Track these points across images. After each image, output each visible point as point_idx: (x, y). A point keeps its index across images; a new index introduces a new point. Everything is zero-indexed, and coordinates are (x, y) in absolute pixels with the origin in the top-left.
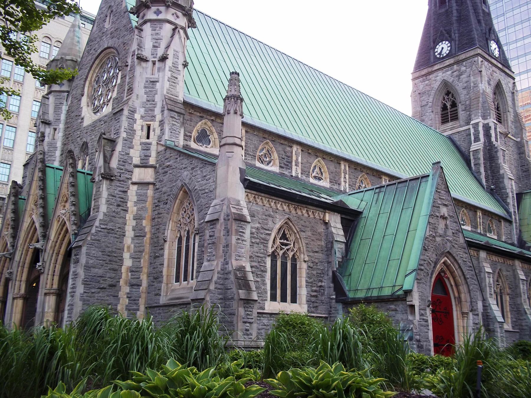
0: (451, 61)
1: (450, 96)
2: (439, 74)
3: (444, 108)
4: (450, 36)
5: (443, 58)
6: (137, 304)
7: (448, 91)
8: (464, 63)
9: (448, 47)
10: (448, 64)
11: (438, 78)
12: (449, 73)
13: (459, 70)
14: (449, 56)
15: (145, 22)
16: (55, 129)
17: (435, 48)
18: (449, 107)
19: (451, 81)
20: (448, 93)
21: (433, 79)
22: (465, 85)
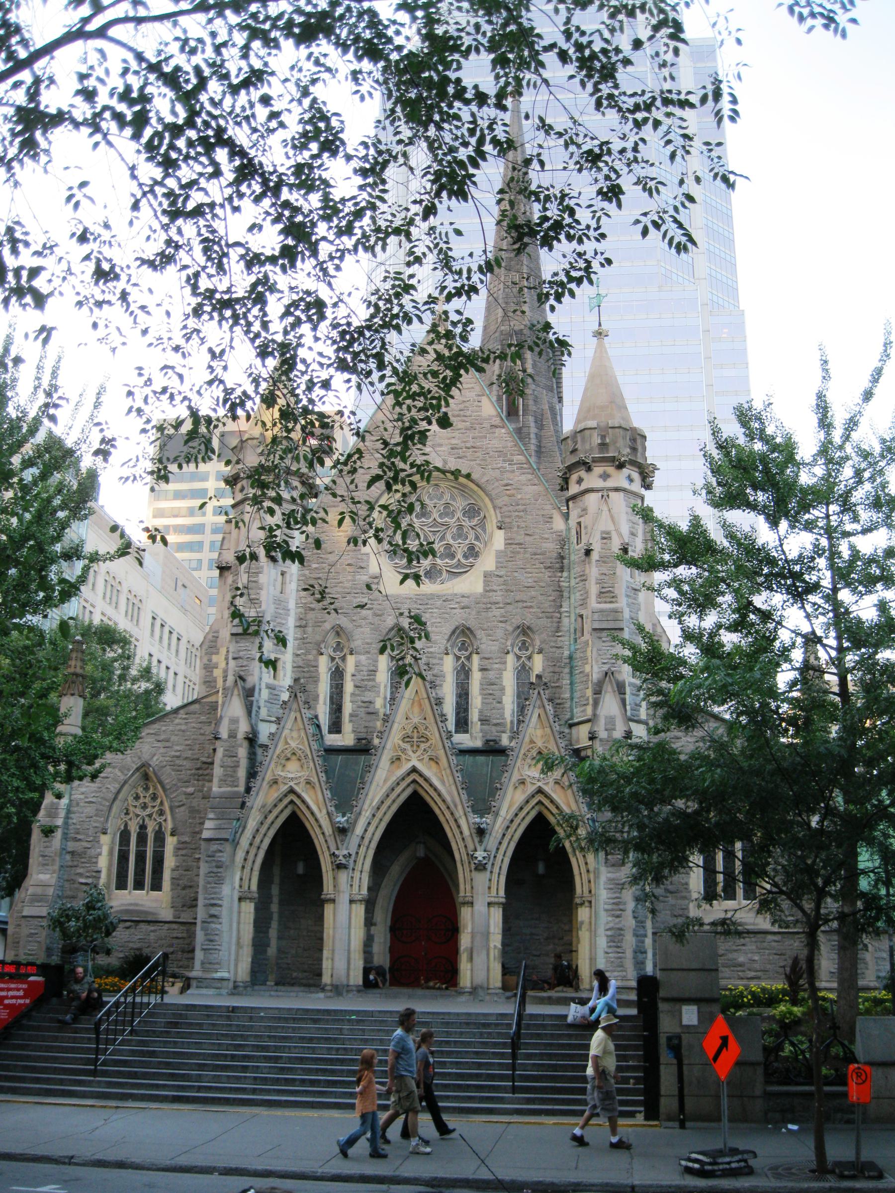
6: (644, 927)
15: (617, 490)
16: (283, 574)
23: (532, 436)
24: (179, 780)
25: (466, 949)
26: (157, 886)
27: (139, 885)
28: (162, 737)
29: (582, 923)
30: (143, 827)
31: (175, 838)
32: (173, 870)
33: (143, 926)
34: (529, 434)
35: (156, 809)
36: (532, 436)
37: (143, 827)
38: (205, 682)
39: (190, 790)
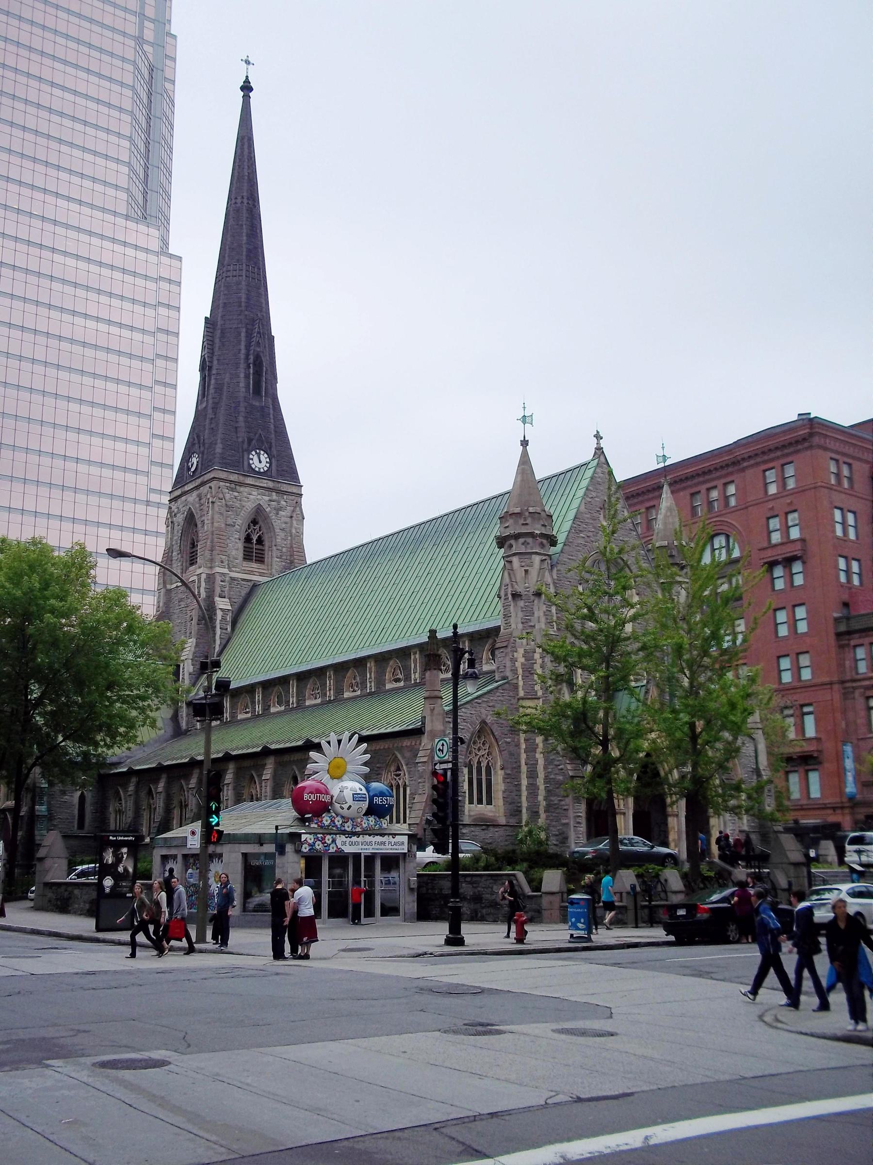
0: (270, 484)
1: (257, 527)
2: (254, 493)
3: (248, 539)
4: (270, 448)
5: (259, 473)
7: (255, 519)
8: (285, 497)
9: (267, 462)
10: (265, 485)
12: (267, 498)
13: (279, 502)
14: (266, 474)
17: (249, 453)
18: (254, 541)
20: (254, 522)
21: (245, 494)
22: (284, 526)
23: (271, 416)
24: (503, 733)
25: (674, 840)
26: (489, 802)
27: (480, 802)
28: (491, 704)
29: (713, 826)
30: (479, 763)
31: (503, 771)
32: (504, 792)
33: (491, 829)
34: (269, 414)
35: (487, 751)
36: (271, 416)
37: (479, 763)
38: (512, 670)
39: (508, 740)
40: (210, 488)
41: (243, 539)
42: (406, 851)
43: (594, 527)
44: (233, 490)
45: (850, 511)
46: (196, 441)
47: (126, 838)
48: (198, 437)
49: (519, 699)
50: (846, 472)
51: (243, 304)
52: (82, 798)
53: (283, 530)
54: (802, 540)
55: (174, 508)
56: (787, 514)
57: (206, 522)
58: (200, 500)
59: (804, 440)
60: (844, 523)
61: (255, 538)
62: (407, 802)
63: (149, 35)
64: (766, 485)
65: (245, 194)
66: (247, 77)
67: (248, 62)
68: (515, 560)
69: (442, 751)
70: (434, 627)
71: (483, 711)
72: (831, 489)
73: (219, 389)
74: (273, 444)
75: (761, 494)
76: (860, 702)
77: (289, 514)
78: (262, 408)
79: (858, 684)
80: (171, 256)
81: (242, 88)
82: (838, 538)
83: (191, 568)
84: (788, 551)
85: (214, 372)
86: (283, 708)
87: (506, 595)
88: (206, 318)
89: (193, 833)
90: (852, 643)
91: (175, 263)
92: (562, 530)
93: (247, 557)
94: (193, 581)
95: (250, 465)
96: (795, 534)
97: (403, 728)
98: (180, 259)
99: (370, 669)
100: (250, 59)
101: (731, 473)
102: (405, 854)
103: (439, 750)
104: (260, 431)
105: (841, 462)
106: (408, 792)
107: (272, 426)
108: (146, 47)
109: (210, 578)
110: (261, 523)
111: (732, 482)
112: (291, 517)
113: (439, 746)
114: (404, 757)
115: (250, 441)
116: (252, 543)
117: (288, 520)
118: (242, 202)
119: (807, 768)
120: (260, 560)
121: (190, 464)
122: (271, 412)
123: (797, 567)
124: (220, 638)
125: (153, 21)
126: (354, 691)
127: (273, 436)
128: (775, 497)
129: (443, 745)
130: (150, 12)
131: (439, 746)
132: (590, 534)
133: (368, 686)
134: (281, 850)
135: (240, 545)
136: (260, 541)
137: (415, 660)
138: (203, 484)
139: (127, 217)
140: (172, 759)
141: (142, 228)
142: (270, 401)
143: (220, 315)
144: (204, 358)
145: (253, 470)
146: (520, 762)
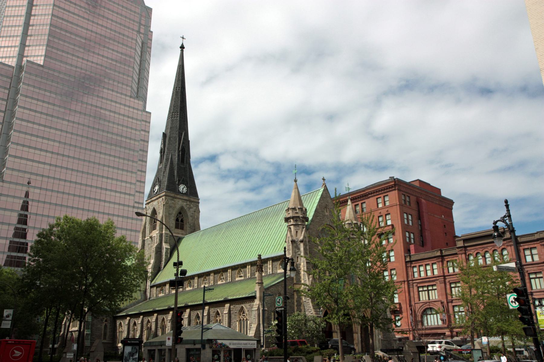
1: (181, 215)
2: (180, 201)
3: (177, 220)
4: (187, 184)
5: (182, 193)
7: (180, 212)
8: (193, 203)
11: (179, 203)
12: (185, 204)
13: (190, 205)
14: (186, 194)
18: (180, 221)
19: (185, 208)
20: (180, 213)
21: (177, 202)
22: (192, 215)
25: (356, 343)
34: (187, 170)
40: (163, 199)
41: (175, 220)
42: (256, 347)
43: (323, 215)
44: (171, 200)
45: (409, 214)
46: (157, 180)
47: (135, 342)
48: (158, 179)
49: (294, 284)
50: (408, 199)
51: (178, 128)
52: (106, 326)
53: (191, 216)
54: (392, 225)
55: (147, 207)
56: (386, 215)
57: (161, 213)
58: (158, 204)
59: (392, 187)
60: (408, 219)
61: (180, 219)
62: (248, 327)
63: (142, 31)
64: (378, 204)
65: (180, 86)
66: (183, 43)
67: (183, 38)
68: (292, 227)
69: (279, 302)
70: (259, 254)
71: (280, 289)
72: (403, 206)
73: (167, 160)
74: (188, 182)
75: (376, 208)
76: (415, 288)
77: (194, 210)
78: (184, 168)
79: (414, 281)
80: (147, 112)
81: (181, 47)
82: (406, 225)
83: (153, 231)
84: (387, 229)
85: (166, 153)
86: (191, 288)
87: (288, 241)
88: (163, 133)
89: (169, 339)
90: (412, 265)
91: (148, 115)
92: (310, 215)
93: (177, 227)
94: (155, 237)
95: (179, 190)
96: (389, 223)
97: (247, 295)
98: (150, 113)
99: (229, 272)
100: (184, 37)
101: (364, 199)
102: (255, 349)
103: (278, 302)
104: (183, 177)
105: (406, 196)
106: (248, 323)
107: (188, 175)
108: (141, 35)
109: (161, 235)
110: (182, 213)
111: (365, 202)
112: (195, 211)
113: (278, 300)
114: (247, 308)
115: (179, 181)
116: (179, 222)
117: (194, 212)
118: (179, 89)
119: (395, 315)
120: (182, 228)
121: (155, 190)
122: (188, 169)
123: (390, 236)
124: (165, 260)
125: (144, 26)
126: (222, 281)
127: (188, 179)
128: (382, 208)
129: (280, 300)
130: (143, 22)
131: (278, 300)
132: (321, 218)
133: (228, 279)
134: (204, 347)
135: (174, 222)
136: (182, 221)
137: (249, 268)
138: (160, 197)
139: (131, 97)
140: (145, 310)
141: (136, 101)
142: (188, 165)
143: (169, 131)
144: (162, 148)
145: (180, 192)
146: (294, 310)
